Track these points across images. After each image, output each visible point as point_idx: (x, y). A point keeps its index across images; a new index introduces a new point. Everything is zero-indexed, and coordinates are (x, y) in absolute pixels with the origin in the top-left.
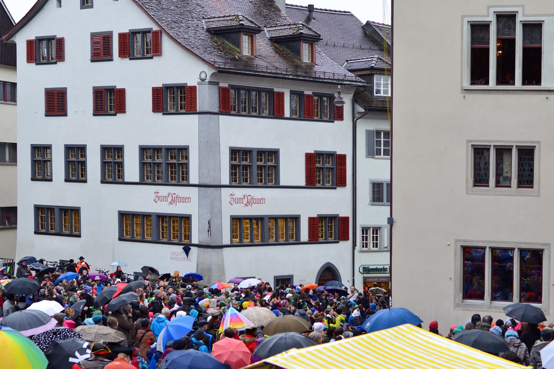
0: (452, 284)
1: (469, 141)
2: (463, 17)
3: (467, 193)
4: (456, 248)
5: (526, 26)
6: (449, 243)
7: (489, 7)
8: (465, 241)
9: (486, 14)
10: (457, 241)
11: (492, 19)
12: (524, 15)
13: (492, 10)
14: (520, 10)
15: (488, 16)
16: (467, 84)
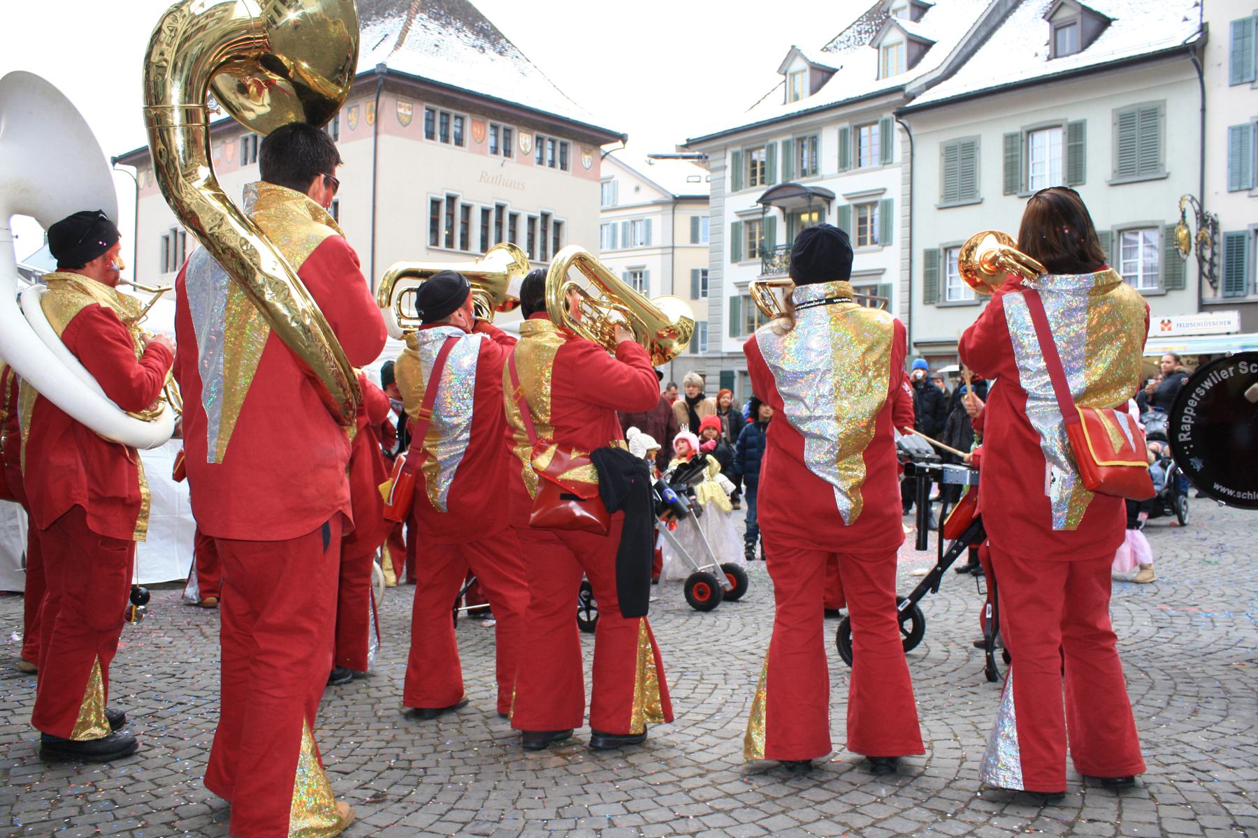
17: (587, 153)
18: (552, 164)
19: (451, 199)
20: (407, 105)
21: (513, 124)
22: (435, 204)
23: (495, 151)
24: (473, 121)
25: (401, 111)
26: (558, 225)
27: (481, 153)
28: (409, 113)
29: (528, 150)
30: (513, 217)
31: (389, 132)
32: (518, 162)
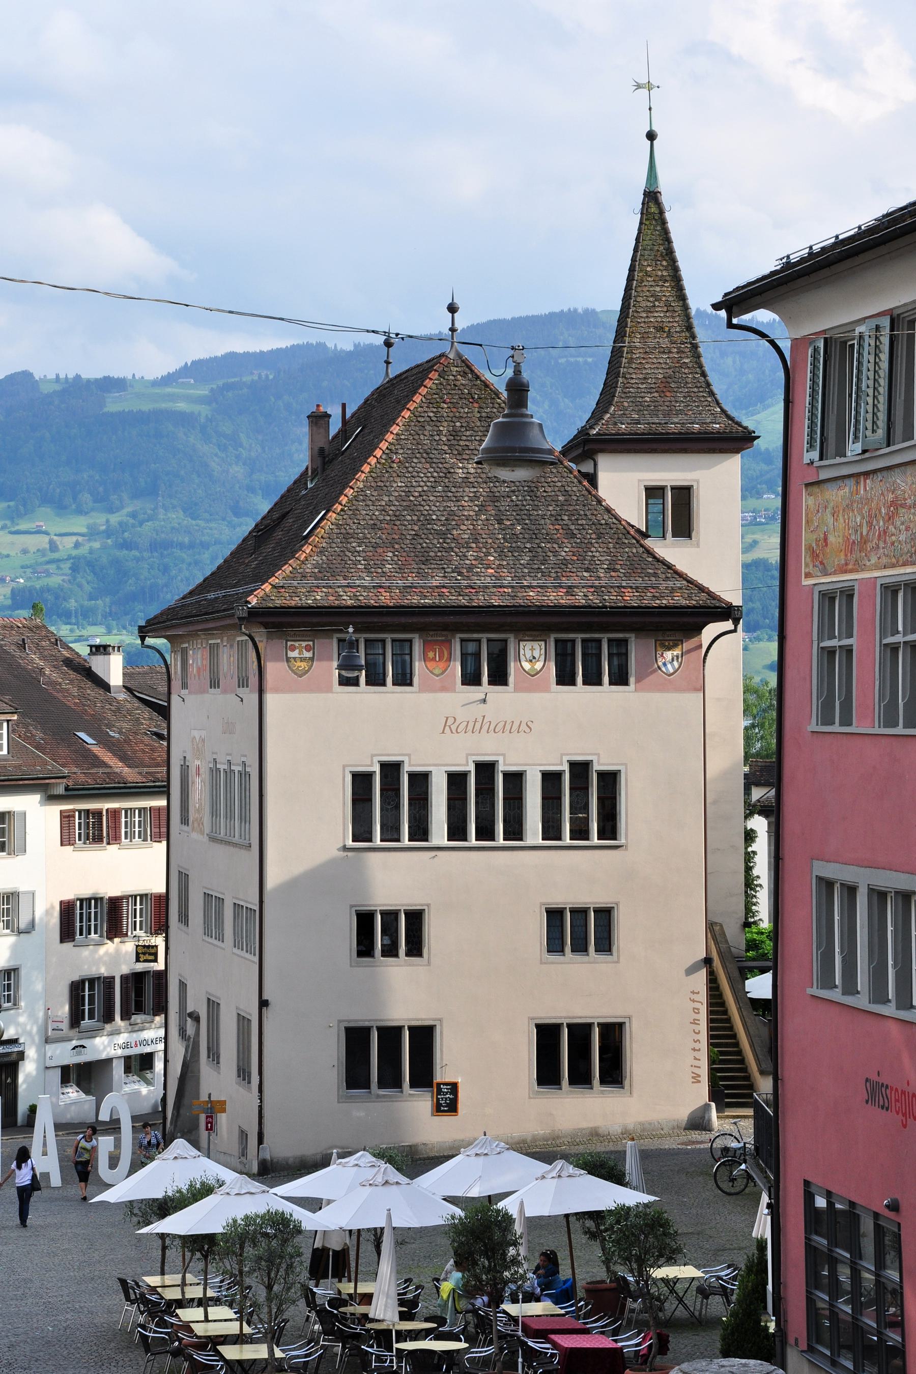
0: (335, 1070)
1: (352, 906)
2: (344, 767)
3: (351, 966)
4: (339, 1030)
5: (413, 776)
6: (331, 1025)
7: (373, 756)
8: (349, 1021)
9: (369, 763)
10: (340, 1021)
11: (377, 769)
12: (410, 765)
13: (376, 759)
14: (405, 759)
15: (371, 765)
16: (350, 843)
17: (669, 648)
18: (593, 679)
19: (391, 770)
20: (304, 644)
21: (505, 631)
22: (361, 781)
23: (471, 679)
24: (427, 645)
25: (295, 654)
26: (610, 780)
27: (444, 689)
28: (308, 655)
29: (538, 666)
30: (515, 780)
31: (277, 690)
32: (516, 690)
